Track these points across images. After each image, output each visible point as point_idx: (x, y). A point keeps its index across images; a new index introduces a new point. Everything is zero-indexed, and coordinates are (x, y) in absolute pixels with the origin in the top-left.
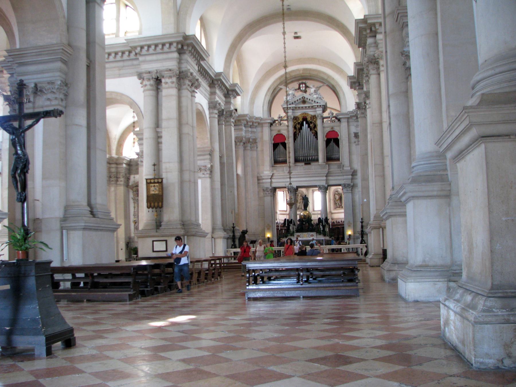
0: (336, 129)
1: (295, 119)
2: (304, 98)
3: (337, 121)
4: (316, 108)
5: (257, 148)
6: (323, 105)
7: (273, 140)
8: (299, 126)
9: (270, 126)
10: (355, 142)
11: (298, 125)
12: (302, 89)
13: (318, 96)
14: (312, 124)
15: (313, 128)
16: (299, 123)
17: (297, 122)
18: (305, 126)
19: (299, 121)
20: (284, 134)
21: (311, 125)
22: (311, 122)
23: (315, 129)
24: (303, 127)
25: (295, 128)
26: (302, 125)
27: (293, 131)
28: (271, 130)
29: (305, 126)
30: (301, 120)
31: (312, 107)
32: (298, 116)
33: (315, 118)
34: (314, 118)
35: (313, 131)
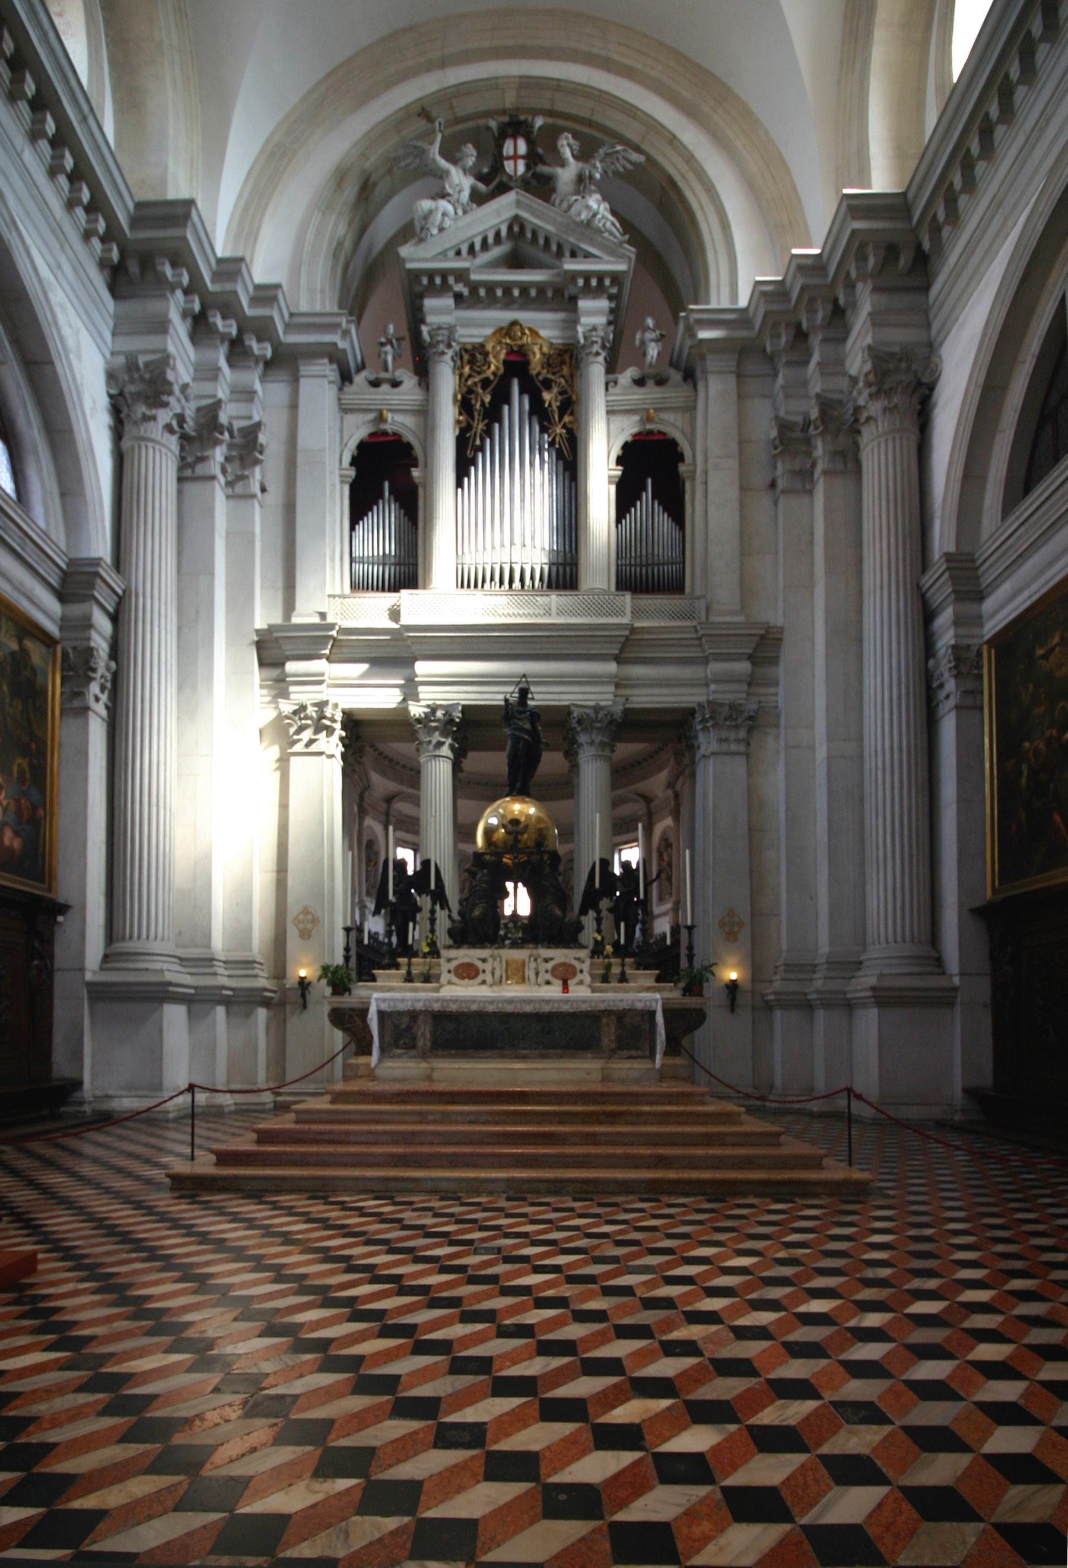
0: (672, 425)
1: (466, 357)
2: (516, 229)
3: (676, 376)
4: (573, 299)
5: (263, 490)
6: (616, 278)
7: (352, 464)
8: (487, 399)
9: (341, 389)
10: (773, 485)
11: (480, 391)
12: (509, 166)
13: (595, 206)
14: (555, 390)
15: (554, 407)
16: (485, 383)
17: (477, 380)
18: (518, 403)
19: (488, 373)
20: (409, 437)
21: (547, 396)
22: (548, 384)
23: (566, 419)
24: (506, 408)
25: (465, 405)
26: (502, 396)
27: (458, 422)
28: (345, 409)
29: (518, 403)
30: (495, 365)
31: (558, 291)
32: (482, 346)
33: (567, 358)
34: (563, 362)
35: (559, 430)
